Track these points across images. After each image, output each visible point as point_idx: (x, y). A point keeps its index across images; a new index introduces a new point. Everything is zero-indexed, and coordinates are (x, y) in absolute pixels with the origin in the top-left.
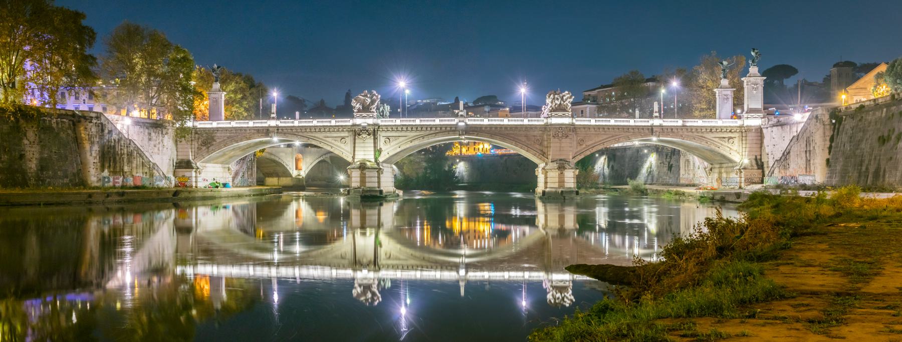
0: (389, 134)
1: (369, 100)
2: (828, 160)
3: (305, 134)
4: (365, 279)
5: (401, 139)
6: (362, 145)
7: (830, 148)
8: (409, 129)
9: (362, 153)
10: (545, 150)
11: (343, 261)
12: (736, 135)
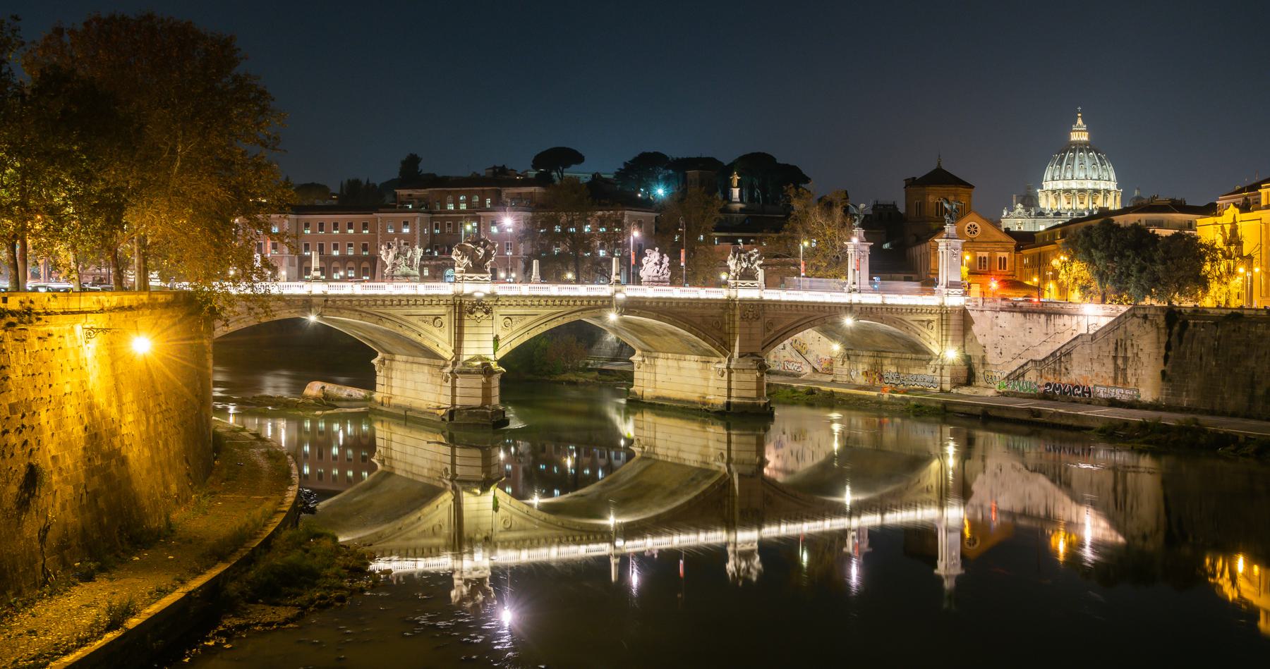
0: (510, 311)
1: (482, 251)
2: (1163, 373)
5: (530, 319)
6: (475, 330)
7: (1166, 358)
8: (550, 303)
9: (475, 344)
10: (726, 339)
12: (935, 317)
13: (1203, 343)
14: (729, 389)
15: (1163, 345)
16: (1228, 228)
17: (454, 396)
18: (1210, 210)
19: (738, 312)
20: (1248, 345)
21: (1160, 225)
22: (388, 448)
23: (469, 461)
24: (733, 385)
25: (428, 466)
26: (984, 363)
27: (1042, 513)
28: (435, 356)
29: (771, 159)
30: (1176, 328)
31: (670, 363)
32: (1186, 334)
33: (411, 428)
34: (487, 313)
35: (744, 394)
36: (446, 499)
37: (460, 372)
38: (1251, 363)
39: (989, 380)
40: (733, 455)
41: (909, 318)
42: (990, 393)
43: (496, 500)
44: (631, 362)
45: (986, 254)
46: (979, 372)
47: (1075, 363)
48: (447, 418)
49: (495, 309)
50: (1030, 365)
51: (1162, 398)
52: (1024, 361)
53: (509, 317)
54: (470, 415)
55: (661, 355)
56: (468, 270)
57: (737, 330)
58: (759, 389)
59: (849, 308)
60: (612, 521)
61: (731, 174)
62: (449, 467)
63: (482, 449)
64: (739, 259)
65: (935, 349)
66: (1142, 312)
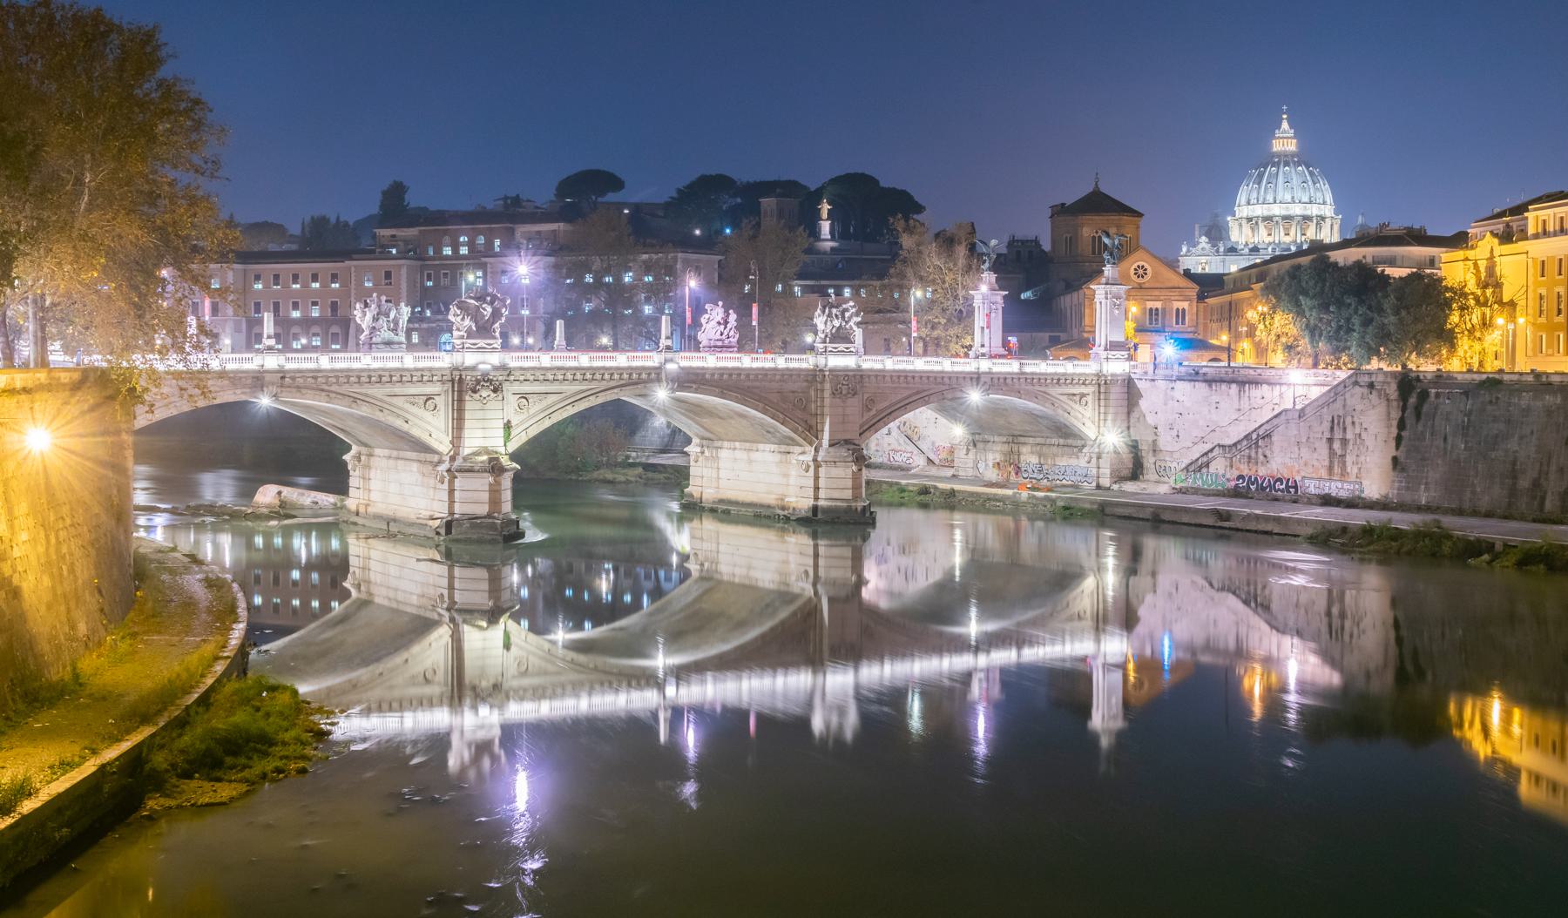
0: (527, 388)
1: (489, 309)
2: (1395, 460)
4: (482, 727)
6: (480, 414)
7: (1399, 440)
8: (579, 376)
9: (480, 433)
10: (813, 422)
11: (427, 690)
12: (1090, 390)
13: (1448, 419)
14: (817, 488)
15: (1395, 423)
16: (1482, 265)
17: (452, 502)
18: (1459, 240)
19: (827, 386)
20: (1508, 422)
21: (1392, 262)
23: (472, 585)
24: (822, 483)
25: (419, 591)
26: (1155, 450)
27: (1232, 645)
28: (425, 448)
29: (871, 180)
30: (1412, 400)
31: (738, 454)
32: (1425, 408)
34: (495, 391)
35: (836, 495)
36: (442, 634)
37: (460, 471)
38: (1513, 445)
39: (1162, 472)
40: (822, 572)
41: (1055, 391)
42: (1163, 489)
43: (507, 635)
44: (687, 454)
45: (1158, 305)
46: (1149, 461)
47: (1276, 448)
48: (443, 531)
49: (506, 386)
50: (1216, 451)
51: (1393, 494)
52: (1208, 447)
53: (524, 396)
54: (474, 526)
55: (726, 444)
56: (470, 335)
57: (827, 410)
58: (856, 487)
59: (976, 378)
61: (819, 202)
62: (446, 592)
63: (489, 568)
64: (830, 315)
65: (1090, 431)
66: (1367, 379)
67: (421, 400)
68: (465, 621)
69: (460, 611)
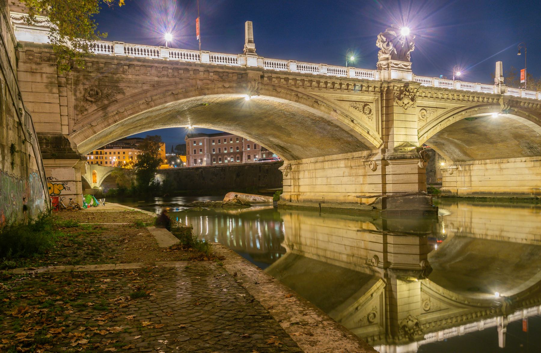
3: (309, 91)
5: (440, 112)
6: (402, 117)
9: (403, 131)
17: (384, 184)
22: (297, 235)
23: (404, 250)
25: (349, 251)
31: (489, 166)
33: (324, 218)
36: (378, 287)
37: (393, 158)
48: (379, 206)
53: (424, 108)
55: (477, 162)
60: (497, 295)
62: (381, 256)
63: (420, 236)
67: (361, 106)
68: (399, 278)
69: (395, 270)
